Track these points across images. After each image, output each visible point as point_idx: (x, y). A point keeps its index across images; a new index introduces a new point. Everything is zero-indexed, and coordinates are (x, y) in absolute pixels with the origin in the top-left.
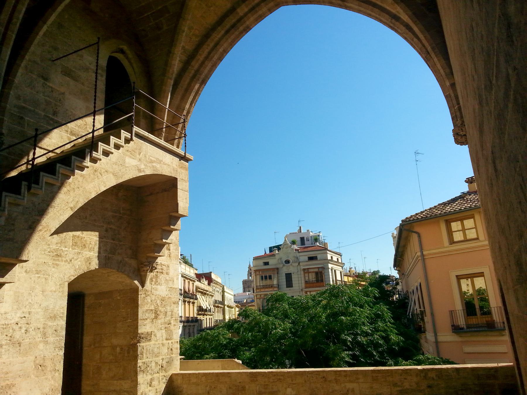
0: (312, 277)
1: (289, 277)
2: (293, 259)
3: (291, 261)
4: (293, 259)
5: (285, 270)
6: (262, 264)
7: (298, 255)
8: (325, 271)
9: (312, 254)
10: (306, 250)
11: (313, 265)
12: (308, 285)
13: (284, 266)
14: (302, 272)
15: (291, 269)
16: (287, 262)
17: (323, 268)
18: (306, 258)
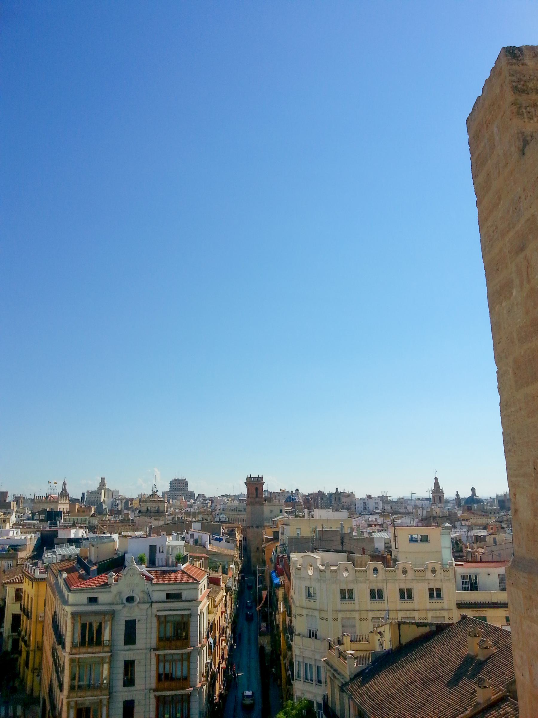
0: (170, 631)
1: (130, 627)
2: (142, 595)
3: (138, 600)
4: (142, 595)
5: (125, 613)
6: (85, 601)
7: (151, 588)
8: (192, 619)
9: (173, 589)
10: (163, 580)
11: (174, 609)
12: (162, 643)
13: (125, 606)
14: (155, 620)
15: (135, 612)
16: (130, 599)
17: (189, 615)
18: (163, 596)
